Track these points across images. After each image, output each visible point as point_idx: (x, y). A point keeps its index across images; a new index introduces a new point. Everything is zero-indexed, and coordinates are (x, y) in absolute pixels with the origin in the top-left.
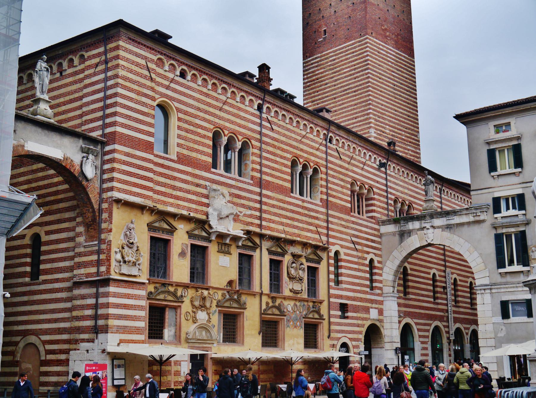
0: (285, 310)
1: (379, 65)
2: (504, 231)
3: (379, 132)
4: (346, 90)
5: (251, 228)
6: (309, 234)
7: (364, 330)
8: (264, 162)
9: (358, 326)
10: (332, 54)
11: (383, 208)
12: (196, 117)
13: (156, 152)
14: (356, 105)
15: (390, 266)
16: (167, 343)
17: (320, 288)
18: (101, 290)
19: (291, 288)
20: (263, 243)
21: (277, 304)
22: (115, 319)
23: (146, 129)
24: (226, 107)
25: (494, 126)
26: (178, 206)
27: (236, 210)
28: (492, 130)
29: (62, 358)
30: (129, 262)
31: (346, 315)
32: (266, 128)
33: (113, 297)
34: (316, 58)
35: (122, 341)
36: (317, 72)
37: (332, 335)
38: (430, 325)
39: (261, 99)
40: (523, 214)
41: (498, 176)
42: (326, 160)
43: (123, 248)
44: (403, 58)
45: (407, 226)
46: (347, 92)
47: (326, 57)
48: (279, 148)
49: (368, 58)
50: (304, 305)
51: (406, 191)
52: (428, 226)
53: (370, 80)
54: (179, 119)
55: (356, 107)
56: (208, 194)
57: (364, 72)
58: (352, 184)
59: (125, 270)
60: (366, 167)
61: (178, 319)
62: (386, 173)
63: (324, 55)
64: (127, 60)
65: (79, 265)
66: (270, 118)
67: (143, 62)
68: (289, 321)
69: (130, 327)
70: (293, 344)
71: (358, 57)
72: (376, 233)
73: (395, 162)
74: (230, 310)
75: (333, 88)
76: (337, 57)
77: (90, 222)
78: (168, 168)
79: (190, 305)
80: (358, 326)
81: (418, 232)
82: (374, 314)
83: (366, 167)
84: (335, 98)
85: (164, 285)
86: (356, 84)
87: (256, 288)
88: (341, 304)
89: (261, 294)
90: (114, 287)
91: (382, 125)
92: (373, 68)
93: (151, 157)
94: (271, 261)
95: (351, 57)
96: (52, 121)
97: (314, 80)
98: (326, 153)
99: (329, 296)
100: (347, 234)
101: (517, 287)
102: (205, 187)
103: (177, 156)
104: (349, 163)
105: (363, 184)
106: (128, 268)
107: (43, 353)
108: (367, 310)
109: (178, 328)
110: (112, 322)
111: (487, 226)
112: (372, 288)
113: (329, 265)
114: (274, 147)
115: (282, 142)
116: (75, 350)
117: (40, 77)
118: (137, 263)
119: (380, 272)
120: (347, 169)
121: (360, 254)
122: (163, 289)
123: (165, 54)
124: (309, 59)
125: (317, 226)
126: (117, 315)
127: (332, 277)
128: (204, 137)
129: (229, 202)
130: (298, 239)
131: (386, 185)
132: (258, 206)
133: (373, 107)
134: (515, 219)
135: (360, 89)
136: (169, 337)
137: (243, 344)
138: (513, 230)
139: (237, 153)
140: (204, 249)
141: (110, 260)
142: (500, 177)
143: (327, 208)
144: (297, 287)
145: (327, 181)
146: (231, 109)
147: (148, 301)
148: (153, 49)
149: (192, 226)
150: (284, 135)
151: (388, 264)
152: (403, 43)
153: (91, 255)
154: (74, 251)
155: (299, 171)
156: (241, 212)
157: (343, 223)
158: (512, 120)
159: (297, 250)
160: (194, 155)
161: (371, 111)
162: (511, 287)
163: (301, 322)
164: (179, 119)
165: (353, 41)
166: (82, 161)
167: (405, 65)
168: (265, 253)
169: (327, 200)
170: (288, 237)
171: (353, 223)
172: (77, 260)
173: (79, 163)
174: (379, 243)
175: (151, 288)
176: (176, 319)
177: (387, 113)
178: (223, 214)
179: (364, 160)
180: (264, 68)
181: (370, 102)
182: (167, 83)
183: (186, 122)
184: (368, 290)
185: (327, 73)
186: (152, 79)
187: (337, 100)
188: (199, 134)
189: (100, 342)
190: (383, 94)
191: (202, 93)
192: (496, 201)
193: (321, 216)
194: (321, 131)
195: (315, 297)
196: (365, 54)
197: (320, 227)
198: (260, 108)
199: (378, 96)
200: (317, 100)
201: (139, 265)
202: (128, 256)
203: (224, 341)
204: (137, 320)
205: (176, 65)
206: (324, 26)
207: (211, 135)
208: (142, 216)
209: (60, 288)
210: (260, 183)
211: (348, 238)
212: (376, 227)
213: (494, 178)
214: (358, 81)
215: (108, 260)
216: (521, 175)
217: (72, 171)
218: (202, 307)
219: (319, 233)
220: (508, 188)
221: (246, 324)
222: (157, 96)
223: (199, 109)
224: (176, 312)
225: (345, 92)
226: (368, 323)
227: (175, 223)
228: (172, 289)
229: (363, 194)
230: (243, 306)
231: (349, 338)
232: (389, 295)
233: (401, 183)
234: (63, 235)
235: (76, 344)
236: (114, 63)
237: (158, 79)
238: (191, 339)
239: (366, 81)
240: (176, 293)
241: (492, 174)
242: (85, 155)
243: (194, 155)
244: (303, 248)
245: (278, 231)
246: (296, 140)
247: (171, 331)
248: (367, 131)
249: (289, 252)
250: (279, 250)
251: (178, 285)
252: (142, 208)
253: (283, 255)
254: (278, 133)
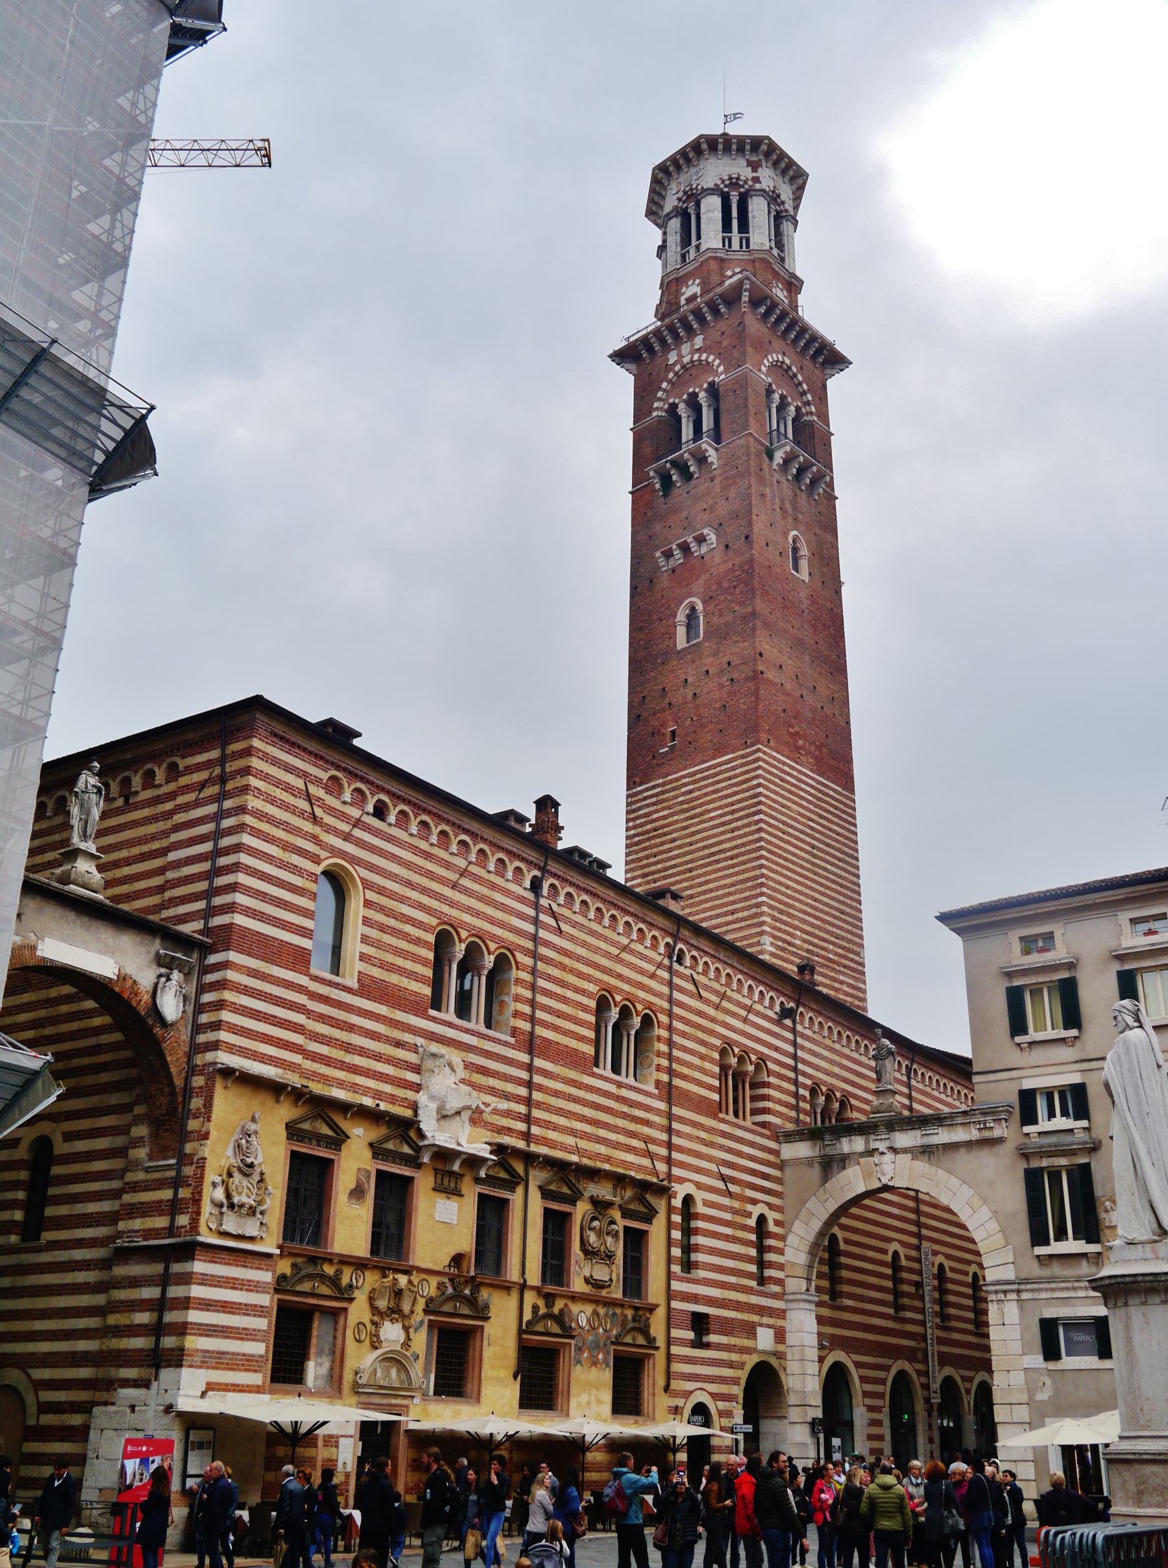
0: (573, 1325)
1: (783, 806)
2: (1045, 1163)
3: (780, 943)
4: (713, 854)
5: (507, 1140)
6: (630, 1158)
7: (743, 1375)
8: (540, 999)
9: (731, 1365)
10: (687, 780)
11: (787, 1105)
12: (402, 899)
13: (313, 970)
14: (733, 885)
15: (802, 1233)
16: (311, 1394)
17: (650, 1276)
18: (176, 1268)
19: (588, 1275)
20: (532, 1173)
21: (556, 1310)
22: (201, 1335)
23: (297, 922)
24: (465, 882)
25: (1021, 939)
26: (354, 1088)
27: (476, 1099)
28: (1017, 948)
29: (74, 1423)
30: (242, 1206)
31: (705, 1339)
32: (547, 927)
33: (200, 1284)
34: (654, 787)
35: (211, 1387)
36: (655, 816)
37: (674, 1384)
38: (887, 1368)
39: (539, 868)
40: (1084, 1129)
41: (1030, 1044)
42: (670, 1000)
43: (230, 1175)
44: (831, 793)
45: (838, 1145)
46: (717, 857)
47: (674, 785)
48: (572, 971)
49: (761, 790)
50: (614, 1314)
51: (836, 1070)
52: (882, 1146)
53: (763, 835)
54: (368, 904)
55: (733, 889)
56: (418, 1062)
57: (750, 819)
58: (723, 1052)
59: (231, 1224)
60: (752, 1017)
61: (339, 1340)
62: (793, 1031)
63: (671, 782)
64: (266, 778)
65: (133, 1211)
66: (555, 908)
67: (299, 783)
69: (233, 1354)
70: (589, 1404)
71: (739, 788)
72: (771, 1158)
73: (814, 1006)
74: (454, 1320)
75: (687, 849)
76: (697, 785)
77: (163, 1115)
78: (339, 1005)
79: (366, 1306)
80: (731, 1365)
81: (862, 1160)
82: (765, 1339)
83: (752, 1017)
84: (690, 870)
85: (313, 1260)
86: (734, 843)
87: (513, 1275)
88: (694, 1314)
89: (523, 1287)
90: (205, 1261)
91: (787, 928)
92: (769, 811)
93: (304, 980)
94: (548, 1214)
95: (726, 788)
96: (100, 897)
97: (647, 832)
98: (670, 984)
99: (670, 1295)
100: (710, 1159)
101: (1074, 1288)
102: (414, 1049)
103: (359, 980)
104: (717, 1007)
105: (746, 1051)
106: (239, 1220)
107: (32, 1409)
108: (750, 1330)
109: (338, 1358)
110: (193, 1342)
111: (1008, 1148)
112: (762, 1281)
113: (670, 1225)
114: (563, 967)
115: (579, 959)
116: (106, 1404)
117: (82, 805)
118: (258, 1210)
119: (779, 1244)
120: (713, 1020)
121: (736, 1204)
122: (311, 1270)
123: (345, 769)
124: (639, 789)
125: (647, 1140)
126: (206, 1325)
127: (676, 1252)
128: (418, 941)
129: (463, 1081)
130: (607, 1167)
131: (795, 1057)
132: (523, 1092)
133: (769, 892)
134: (1069, 1139)
135: (743, 854)
136: (316, 1378)
137: (478, 1400)
138: (1063, 1161)
139: (484, 979)
140: (406, 1183)
141: (200, 1200)
142: (1033, 1046)
143: (670, 1102)
144: (601, 1273)
145: (670, 1043)
146: (476, 887)
147: (276, 1297)
148: (322, 758)
149: (383, 1131)
150: (584, 944)
151: (798, 1227)
152: (831, 762)
153: (159, 1189)
154: (122, 1178)
155: (613, 1021)
156: (487, 1105)
157: (703, 1135)
158: (1057, 928)
159: (604, 1191)
160: (394, 978)
161: (764, 899)
162: (1062, 1289)
164: (368, 904)
165: (731, 756)
166: (156, 985)
167: (836, 808)
168: (535, 1196)
169: (670, 1083)
170: (586, 1161)
171: (724, 1135)
172: (127, 1198)
173: (150, 989)
174: (778, 1181)
175: (285, 1267)
176: (335, 1338)
177: (797, 904)
178: (448, 1107)
179: (748, 1002)
180: (547, 805)
181: (763, 880)
182: (345, 828)
183: (382, 909)
184: (753, 1284)
185: (676, 818)
186: (315, 819)
187: (694, 873)
188: (406, 936)
189: (163, 1387)
190: (790, 865)
191: (416, 851)
192: (1027, 1098)
193: (657, 1119)
194: (660, 939)
195: (639, 1296)
196: (755, 782)
197: (654, 1141)
198: (536, 886)
199: (779, 869)
200: (652, 873)
201: (262, 1213)
202: (240, 1194)
203: (436, 1393)
204: (248, 1339)
205: (367, 792)
206: (671, 723)
207: (431, 938)
208: (277, 1106)
209: (84, 1261)
210: (530, 1044)
211: (714, 1167)
212: (772, 1145)
213: (1021, 1049)
214: (740, 837)
215: (197, 1201)
216: (1078, 1044)
217: (134, 1004)
218: (393, 1312)
219: (650, 1155)
220: (1051, 1071)
221: (488, 1353)
222: (323, 854)
223: (409, 884)
224: (336, 1323)
225: (712, 859)
226: (752, 1360)
227: (345, 1125)
228: (329, 1270)
229: (746, 1073)
230: (482, 1313)
231: (711, 1394)
232: (799, 1297)
233: (826, 1053)
234: (102, 1143)
235: (108, 1390)
236: (239, 782)
237: (329, 820)
238: (364, 1386)
239: (756, 836)
240: (340, 1279)
241: (1018, 1039)
242: (163, 970)
243: (394, 978)
244: (615, 1188)
245: (564, 1148)
246: (608, 955)
247: (321, 1365)
248: (755, 940)
249: (587, 1194)
250: (565, 1190)
251: (346, 1261)
252: (275, 1089)
253: (572, 1201)
254: (572, 939)
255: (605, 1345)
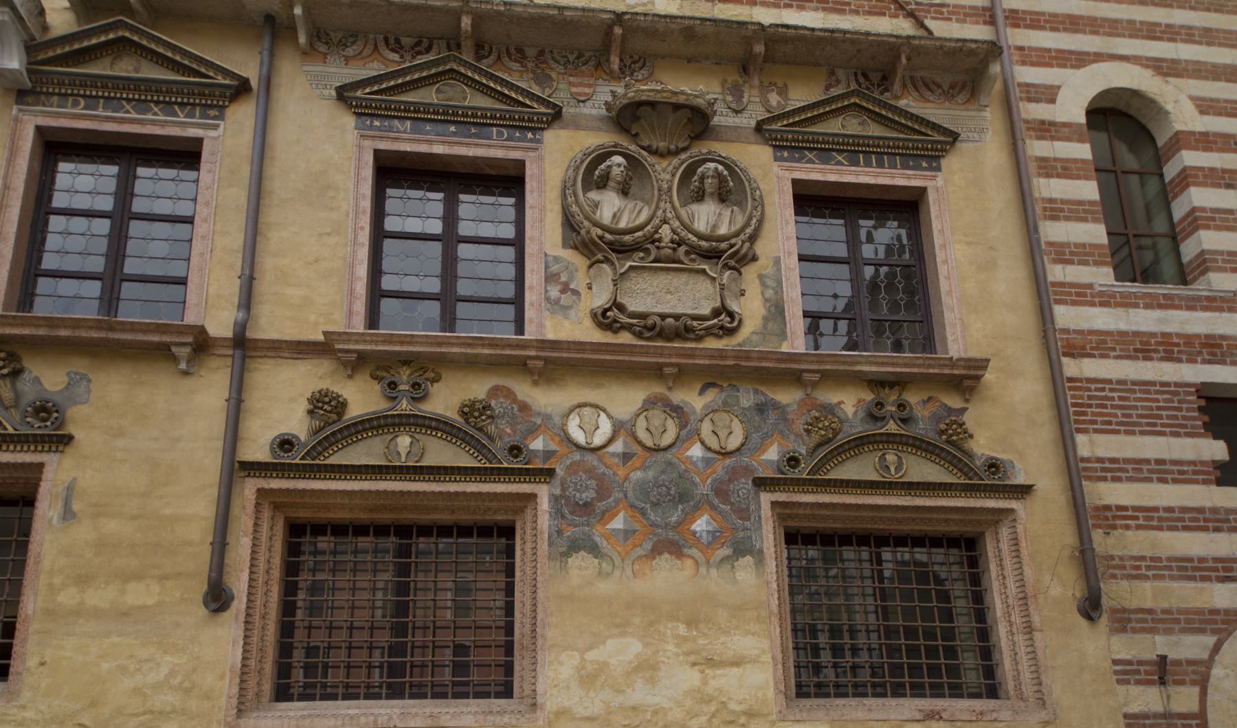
19: (600, 298)
21: (445, 399)
37: (1117, 592)
68: (587, 507)
70: (646, 668)
163: (744, 514)
255: (721, 491)
